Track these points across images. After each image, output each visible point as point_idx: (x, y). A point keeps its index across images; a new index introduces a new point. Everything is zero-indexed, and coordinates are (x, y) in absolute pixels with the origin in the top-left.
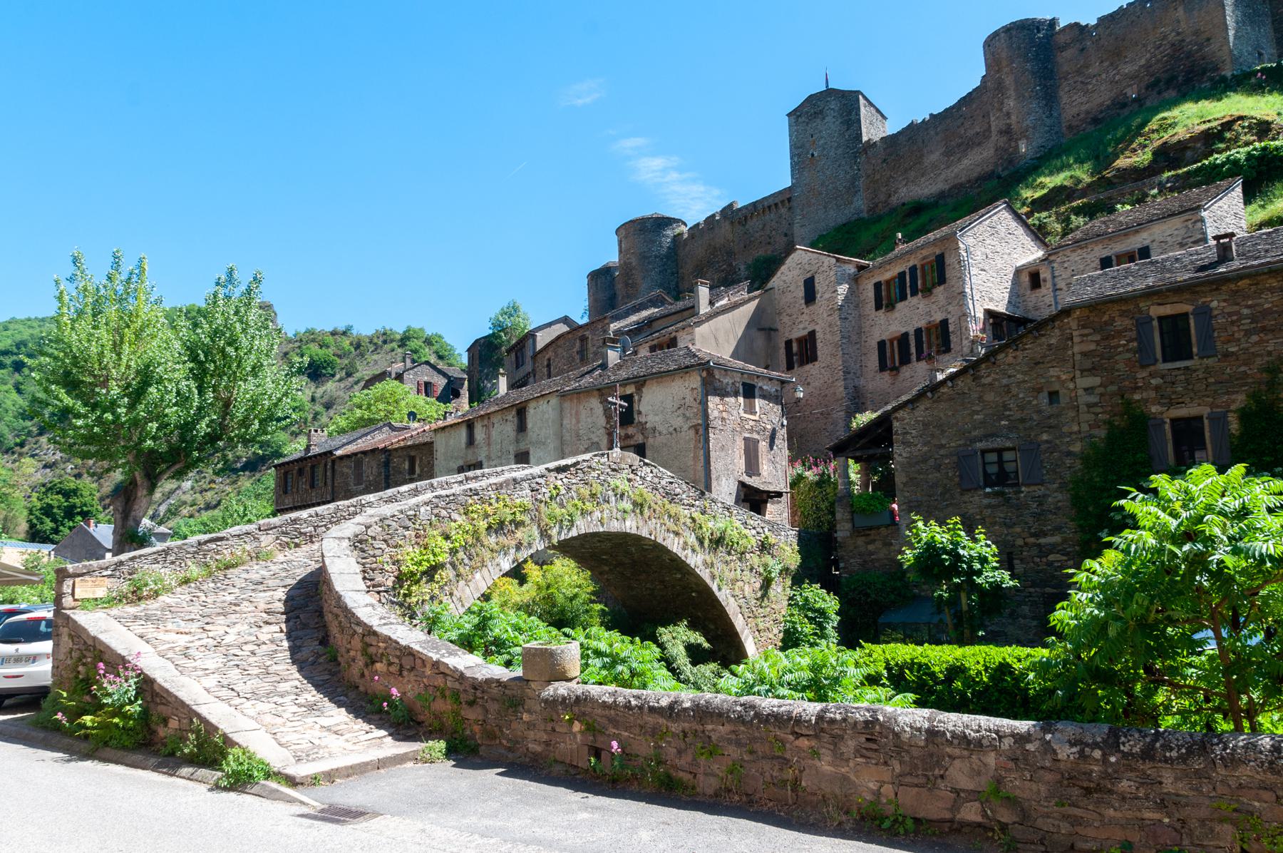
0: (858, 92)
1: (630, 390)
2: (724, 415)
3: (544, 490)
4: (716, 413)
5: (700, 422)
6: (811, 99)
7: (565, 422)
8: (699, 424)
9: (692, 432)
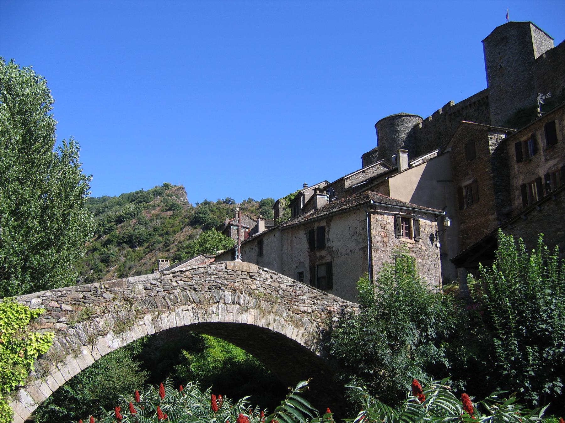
0: (529, 22)
1: (323, 224)
2: (385, 240)
3: (157, 289)
4: (378, 238)
6: (498, 30)
7: (284, 249)
9: (361, 252)
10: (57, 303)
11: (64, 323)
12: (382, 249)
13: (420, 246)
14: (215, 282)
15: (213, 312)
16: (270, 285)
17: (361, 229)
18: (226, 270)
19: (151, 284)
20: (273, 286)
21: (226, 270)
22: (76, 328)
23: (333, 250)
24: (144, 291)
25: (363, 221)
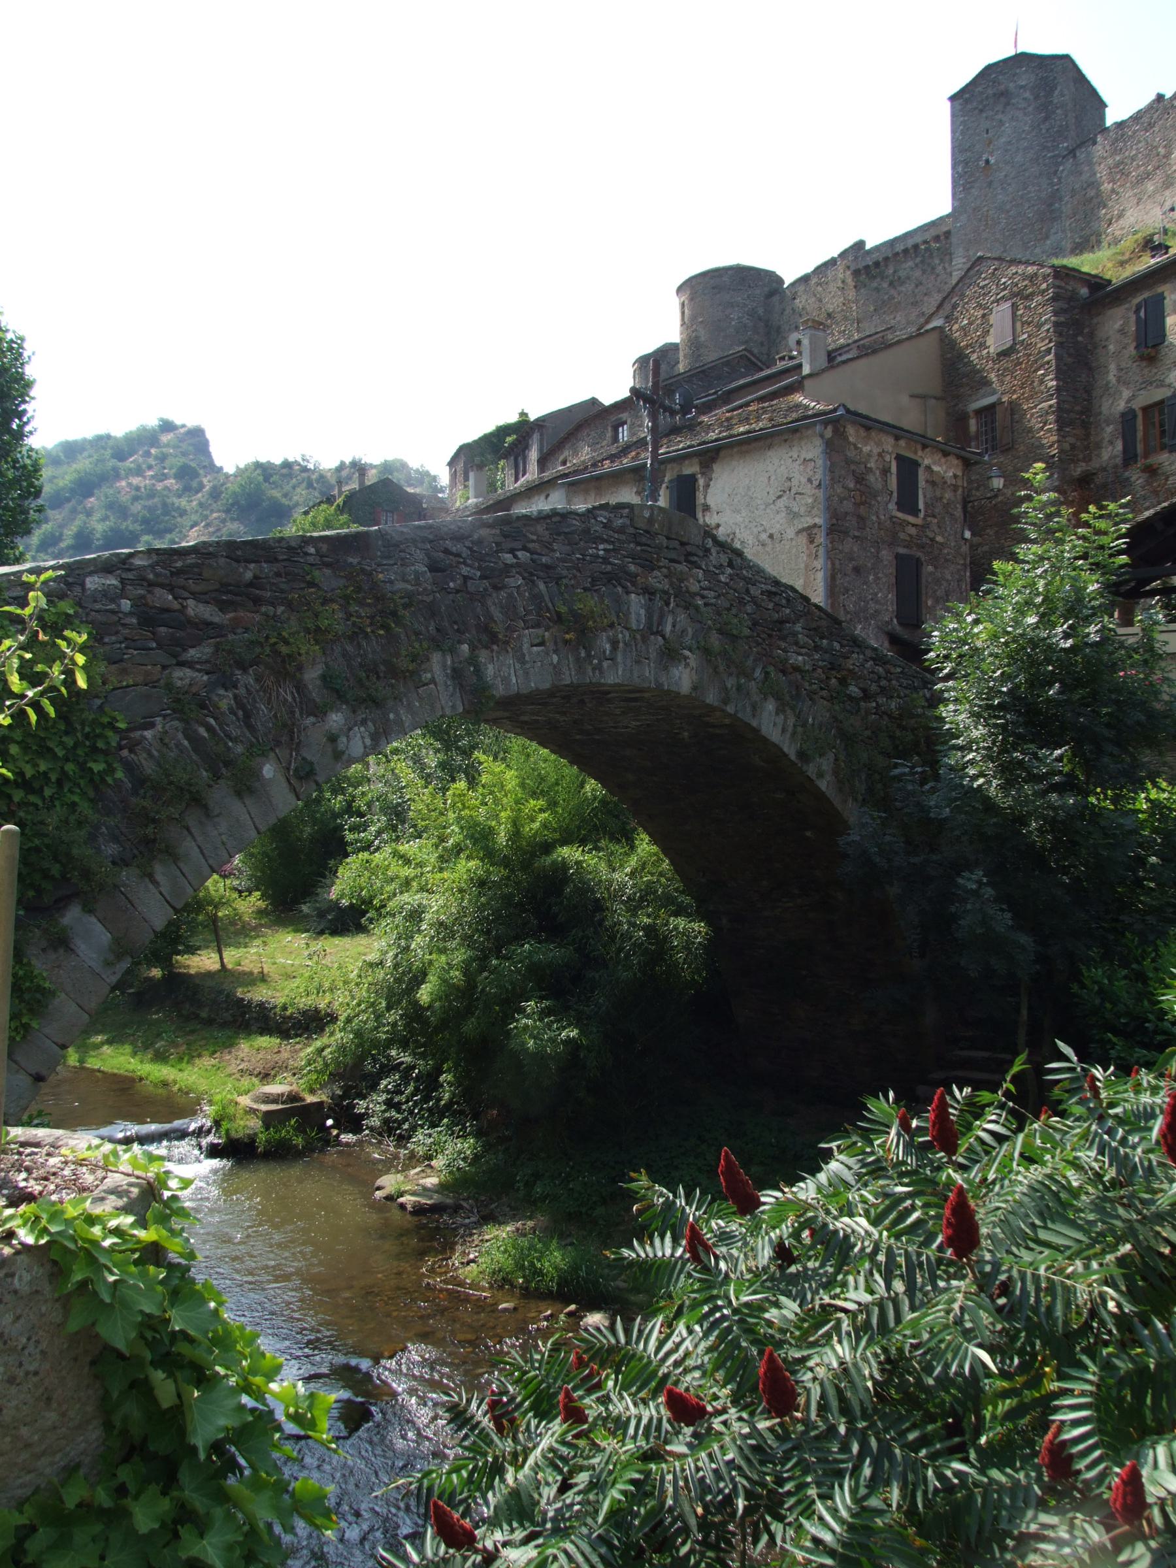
1: (690, 469)
2: (862, 510)
3: (465, 570)
5: (818, 521)
8: (815, 525)
9: (803, 539)
10: (170, 597)
11: (198, 666)
12: (857, 534)
13: (931, 535)
15: (604, 652)
16: (727, 584)
17: (804, 480)
18: (632, 530)
19: (447, 551)
20: (735, 590)
21: (632, 530)
22: (235, 687)
25: (811, 460)
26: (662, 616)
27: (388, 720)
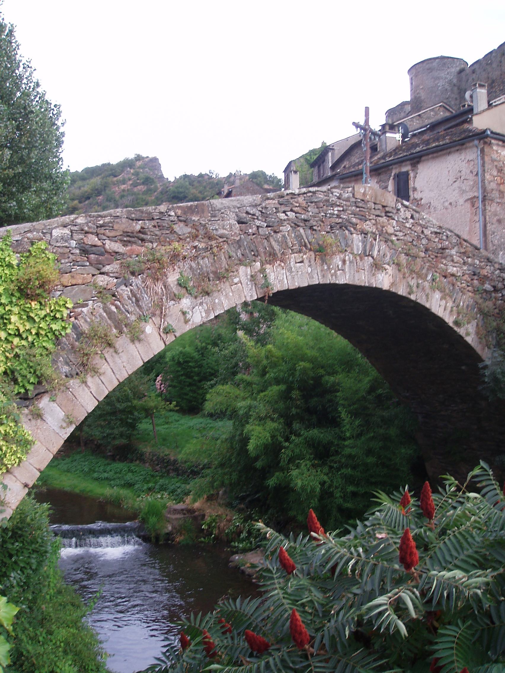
3: (258, 223)
4: (493, 185)
8: (475, 197)
9: (468, 205)
10: (97, 239)
11: (112, 275)
12: (498, 201)
14: (338, 216)
15: (338, 266)
16: (410, 228)
18: (354, 200)
19: (247, 213)
20: (415, 232)
21: (354, 200)
22: (131, 285)
23: (422, 203)
24: (237, 225)
26: (372, 246)
27: (215, 303)
